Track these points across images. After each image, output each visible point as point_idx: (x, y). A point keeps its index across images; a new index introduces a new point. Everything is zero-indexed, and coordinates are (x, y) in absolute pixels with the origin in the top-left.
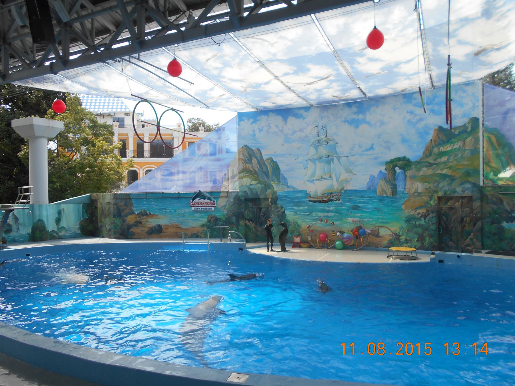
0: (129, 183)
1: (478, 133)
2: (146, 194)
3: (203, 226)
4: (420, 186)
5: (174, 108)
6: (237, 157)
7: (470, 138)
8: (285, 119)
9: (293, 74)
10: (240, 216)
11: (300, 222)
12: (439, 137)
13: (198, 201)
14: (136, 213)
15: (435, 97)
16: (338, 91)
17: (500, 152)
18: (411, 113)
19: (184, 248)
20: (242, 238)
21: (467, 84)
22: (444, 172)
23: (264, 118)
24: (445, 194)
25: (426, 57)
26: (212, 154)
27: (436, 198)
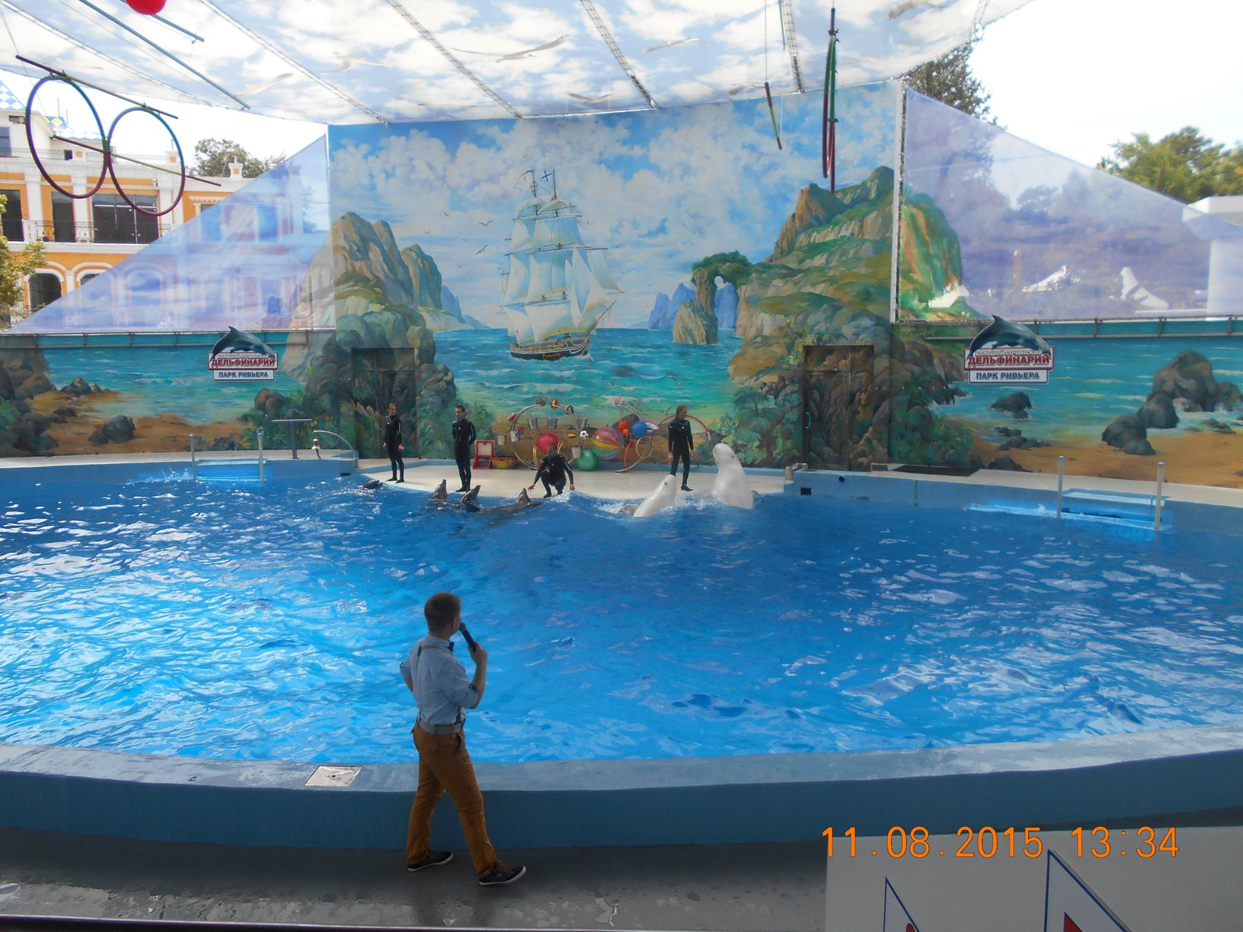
0: (34, 311)
1: (892, 203)
2: (86, 337)
3: (245, 418)
4: (766, 322)
5: (149, 104)
6: (329, 242)
7: (874, 214)
8: (452, 148)
9: (469, 26)
10: (341, 393)
11: (490, 406)
12: (809, 208)
13: (228, 356)
14: (59, 388)
15: (803, 113)
16: (582, 80)
17: (932, 250)
18: (752, 148)
19: (196, 474)
20: (347, 448)
21: (872, 88)
22: (819, 289)
23: (397, 142)
24: (819, 339)
25: (785, 10)
26: (265, 235)
27: (801, 350)
